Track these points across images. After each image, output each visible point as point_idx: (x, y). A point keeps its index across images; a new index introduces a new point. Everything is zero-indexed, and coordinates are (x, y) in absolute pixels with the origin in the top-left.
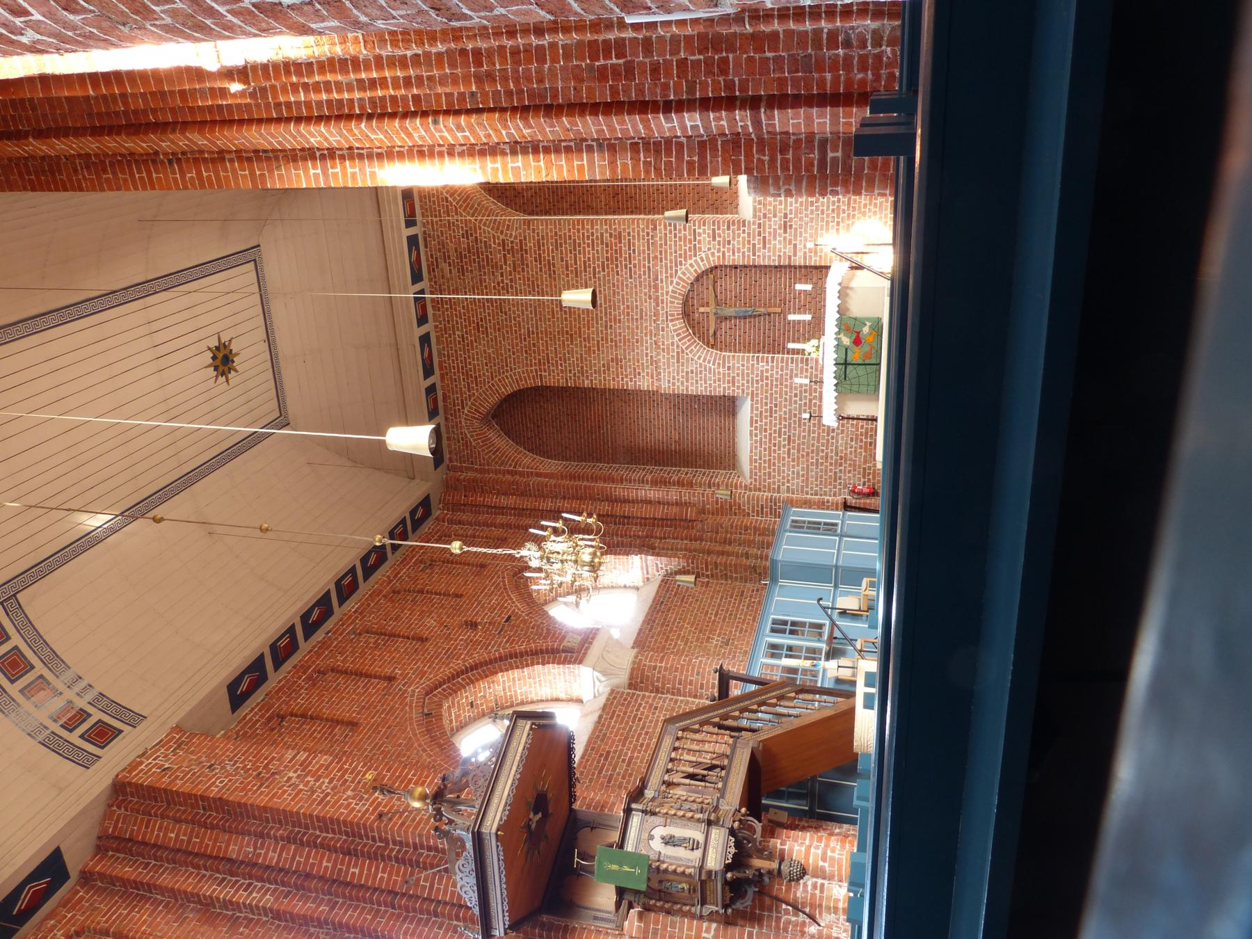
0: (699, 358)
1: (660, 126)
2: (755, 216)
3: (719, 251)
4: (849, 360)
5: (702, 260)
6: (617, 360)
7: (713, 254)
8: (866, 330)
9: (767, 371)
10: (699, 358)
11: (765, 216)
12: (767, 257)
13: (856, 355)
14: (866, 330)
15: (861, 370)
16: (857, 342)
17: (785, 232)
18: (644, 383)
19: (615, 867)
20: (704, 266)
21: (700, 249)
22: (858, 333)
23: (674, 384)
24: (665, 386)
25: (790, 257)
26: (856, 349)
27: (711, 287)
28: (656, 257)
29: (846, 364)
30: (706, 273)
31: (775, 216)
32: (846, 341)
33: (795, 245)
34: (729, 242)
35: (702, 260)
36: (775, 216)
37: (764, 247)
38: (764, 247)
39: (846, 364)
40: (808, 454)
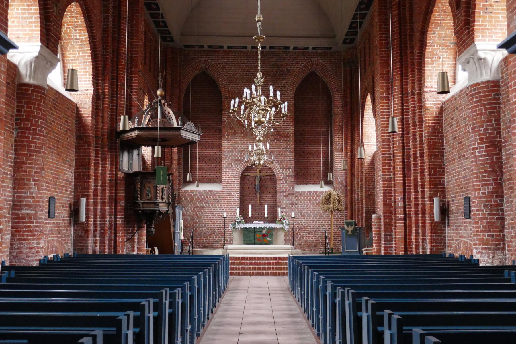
0: (238, 169)
1: (399, 196)
2: (296, 192)
3: (283, 178)
4: (253, 233)
5: (279, 171)
6: (235, 133)
7: (281, 175)
8: (269, 239)
9: (233, 197)
10: (238, 169)
11: (296, 196)
12: (280, 197)
13: (258, 236)
14: (269, 239)
15: (253, 238)
16: (264, 236)
17: (290, 204)
18: (225, 145)
19: (162, 173)
20: (276, 172)
21: (283, 170)
22: (267, 236)
23: (226, 158)
24: (225, 154)
25: (280, 206)
26: (261, 236)
27: (267, 174)
28: (280, 152)
29: (255, 232)
30: (273, 172)
31: (296, 200)
32: (264, 232)
33: (285, 208)
34: (286, 182)
35: (279, 171)
36: (296, 200)
37: (284, 196)
38: (284, 196)
39: (255, 232)
40: (197, 215)
